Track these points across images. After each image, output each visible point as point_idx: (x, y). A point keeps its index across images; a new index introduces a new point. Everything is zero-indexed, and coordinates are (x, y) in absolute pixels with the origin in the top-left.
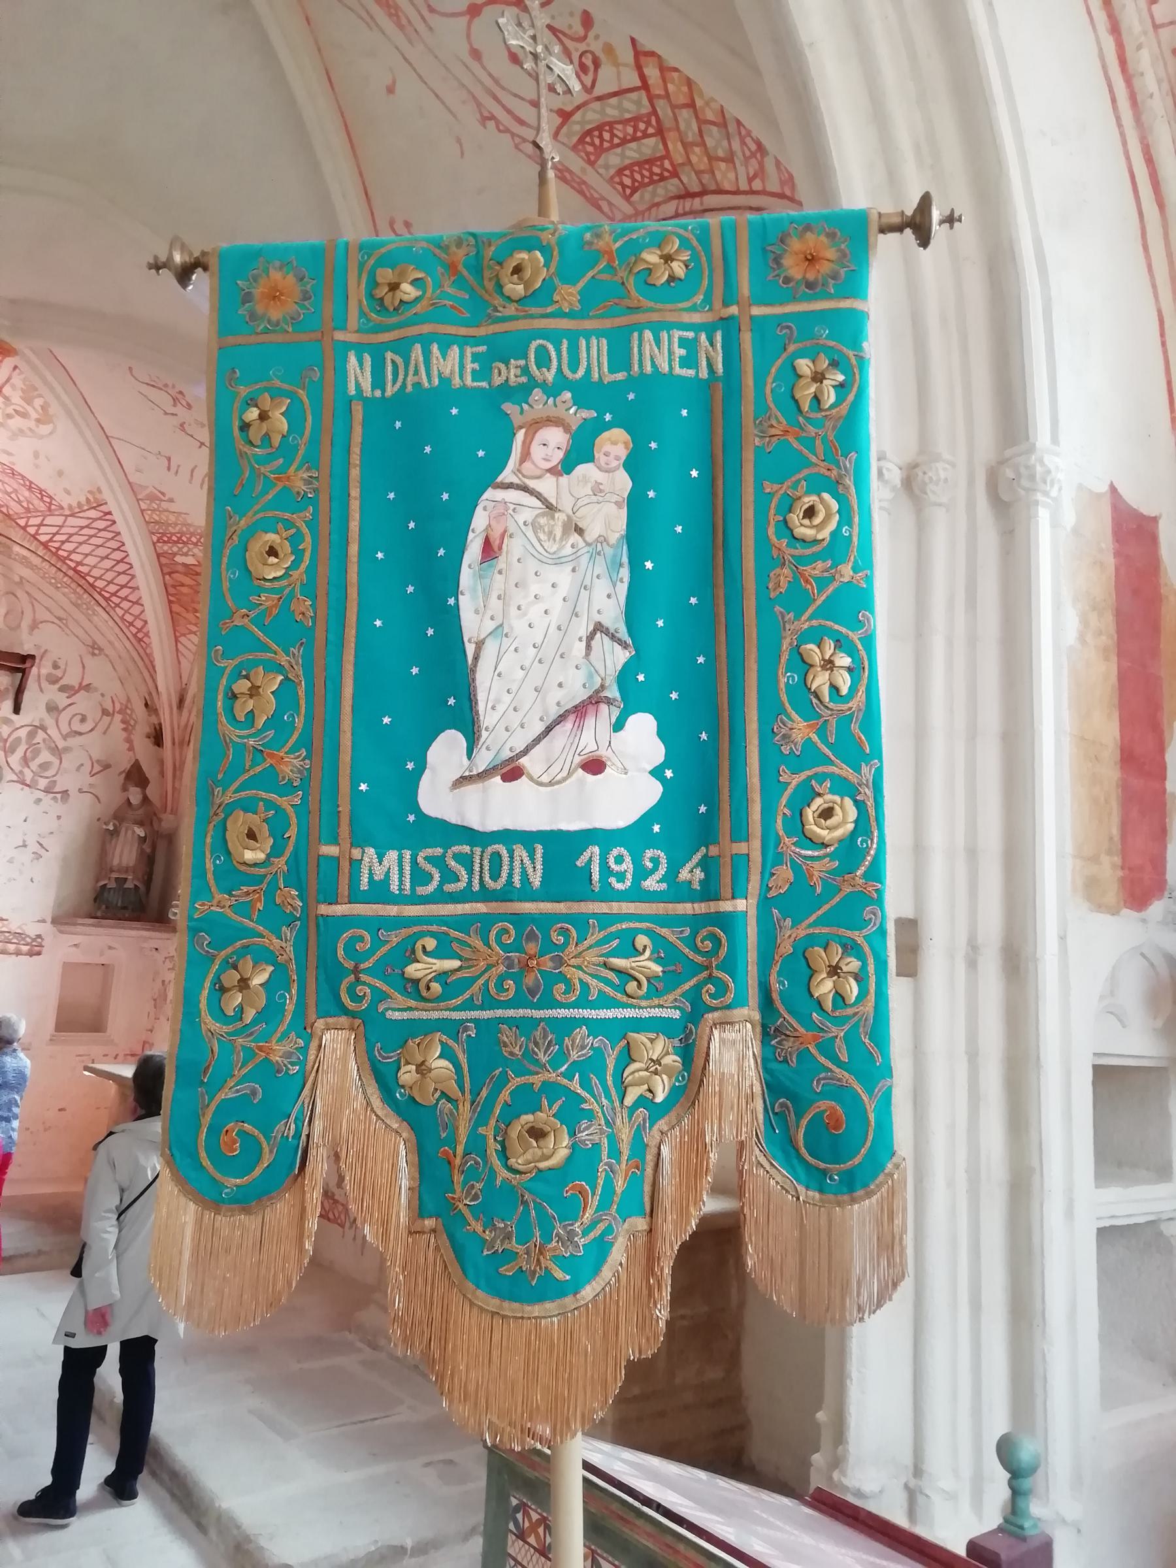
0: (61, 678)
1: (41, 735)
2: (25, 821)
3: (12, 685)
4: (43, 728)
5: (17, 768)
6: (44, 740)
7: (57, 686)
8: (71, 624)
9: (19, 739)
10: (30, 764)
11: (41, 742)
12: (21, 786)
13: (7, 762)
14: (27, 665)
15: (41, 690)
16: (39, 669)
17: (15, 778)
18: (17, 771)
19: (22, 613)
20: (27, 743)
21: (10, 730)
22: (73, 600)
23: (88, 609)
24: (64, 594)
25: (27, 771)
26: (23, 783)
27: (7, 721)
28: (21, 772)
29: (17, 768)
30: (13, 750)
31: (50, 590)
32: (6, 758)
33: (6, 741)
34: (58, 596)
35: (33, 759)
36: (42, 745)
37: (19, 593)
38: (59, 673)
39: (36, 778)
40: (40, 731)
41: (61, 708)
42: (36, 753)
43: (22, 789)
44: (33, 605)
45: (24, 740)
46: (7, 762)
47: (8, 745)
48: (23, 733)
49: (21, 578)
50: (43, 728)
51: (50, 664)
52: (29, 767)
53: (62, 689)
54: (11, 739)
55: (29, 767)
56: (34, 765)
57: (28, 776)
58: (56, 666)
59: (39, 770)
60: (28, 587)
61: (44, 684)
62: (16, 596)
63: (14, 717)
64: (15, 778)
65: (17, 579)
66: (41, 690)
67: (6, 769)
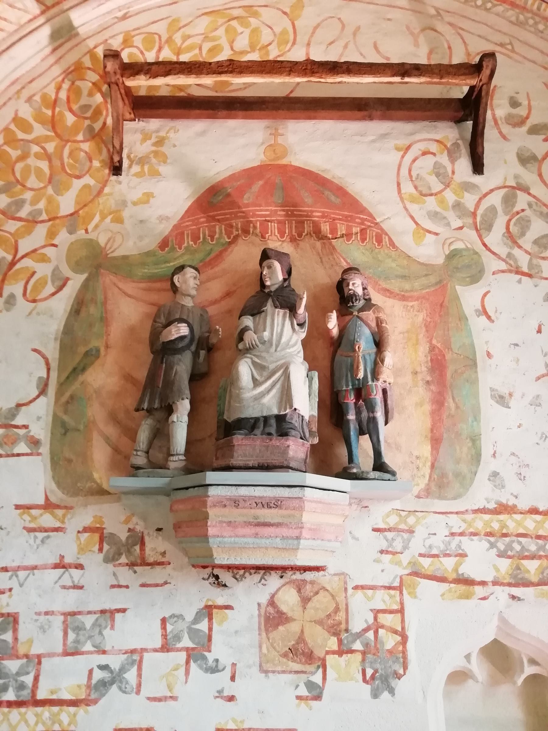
0: (527, 118)
1: (522, 200)
2: (539, 331)
3: (462, 138)
4: (526, 190)
5: (503, 251)
6: (530, 205)
7: (525, 129)
8: (518, 47)
9: (492, 210)
10: (520, 242)
11: (526, 207)
12: (518, 277)
13: (485, 245)
14: (486, 72)
15: (504, 137)
16: (492, 110)
17: (503, 266)
18: (504, 256)
19: (450, 48)
20: (506, 214)
21: (477, 198)
22: (513, 19)
23: (536, 23)
24: (498, 15)
25: (516, 252)
26: (518, 272)
27: (467, 187)
28: (509, 255)
29: (503, 251)
30: (489, 228)
31: (481, 15)
32: (480, 236)
33: (474, 214)
34: (491, 19)
35: (523, 234)
36: (528, 212)
37: (440, 27)
38: (522, 111)
39: (535, 261)
40: (518, 192)
41: (540, 157)
42: (525, 224)
43: (520, 281)
44: (462, 39)
45: (500, 209)
46: (485, 245)
47: (478, 219)
48: (496, 199)
49: (437, 9)
50: (526, 190)
51: (505, 102)
52: (520, 247)
53: (534, 130)
54: (480, 212)
55: (520, 247)
56: (527, 242)
57: (524, 261)
58: (514, 103)
59: (536, 249)
60: (448, 18)
61: (506, 129)
62: (436, 31)
63: (477, 179)
64: (503, 266)
65: (433, 12)
66: (504, 137)
67: (486, 256)
